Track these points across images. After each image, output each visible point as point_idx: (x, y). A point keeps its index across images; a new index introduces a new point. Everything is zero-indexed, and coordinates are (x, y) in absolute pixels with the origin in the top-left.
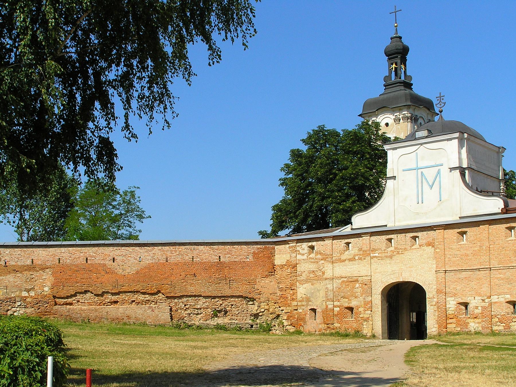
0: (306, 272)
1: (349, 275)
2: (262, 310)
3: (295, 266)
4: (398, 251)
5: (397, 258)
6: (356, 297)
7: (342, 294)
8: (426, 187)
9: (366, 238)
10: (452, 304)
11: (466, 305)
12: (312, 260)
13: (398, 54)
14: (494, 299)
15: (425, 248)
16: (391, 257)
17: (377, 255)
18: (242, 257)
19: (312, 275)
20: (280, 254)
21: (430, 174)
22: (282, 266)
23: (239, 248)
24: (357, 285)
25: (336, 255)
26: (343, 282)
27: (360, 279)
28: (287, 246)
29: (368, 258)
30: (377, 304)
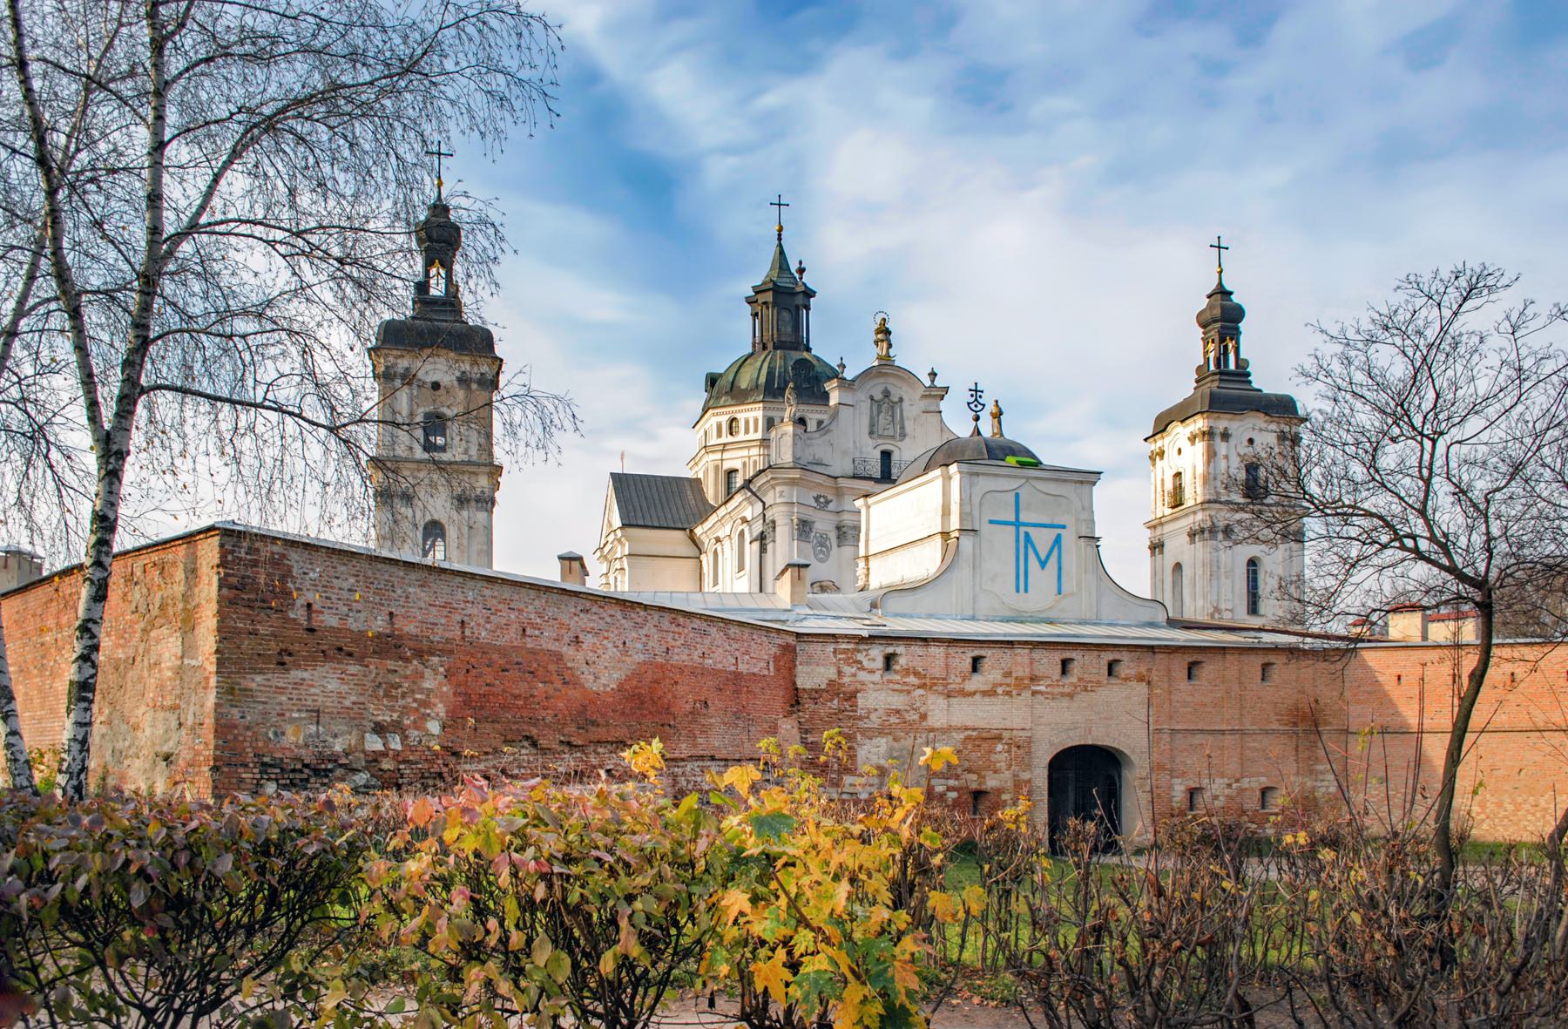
0: (881, 712)
1: (982, 724)
4: (1086, 687)
5: (1082, 698)
6: (995, 772)
7: (967, 765)
8: (1033, 563)
9: (1023, 652)
10: (1179, 791)
12: (896, 687)
14: (1245, 783)
15: (1134, 684)
16: (1071, 696)
17: (1042, 688)
19: (894, 720)
20: (808, 664)
21: (1043, 539)
22: (816, 694)
24: (1000, 747)
25: (955, 682)
26: (968, 738)
27: (1006, 734)
28: (830, 648)
29: (1027, 694)
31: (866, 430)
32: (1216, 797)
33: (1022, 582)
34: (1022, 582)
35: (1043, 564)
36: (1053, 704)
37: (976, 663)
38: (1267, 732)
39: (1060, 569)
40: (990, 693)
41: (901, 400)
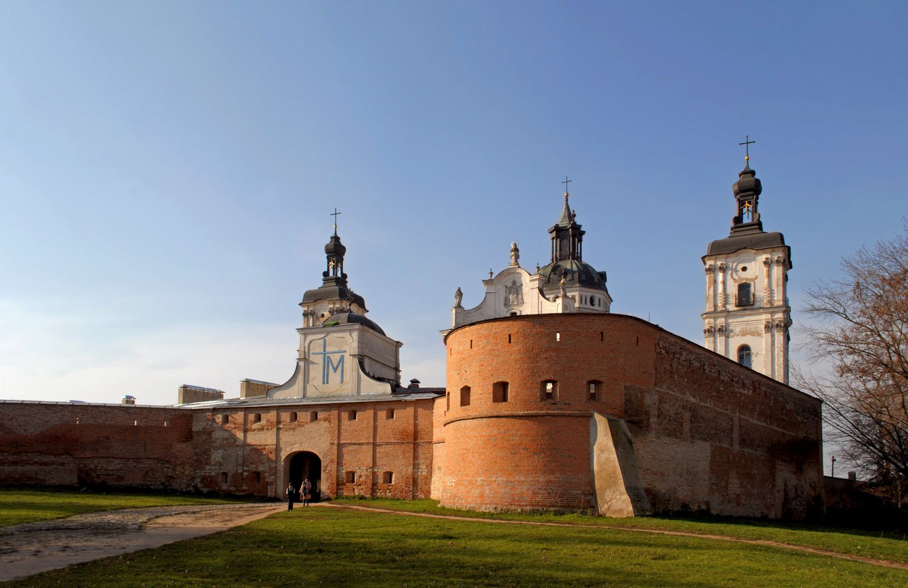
3: (210, 433)
5: (298, 430)
8: (331, 369)
11: (353, 473)
13: (336, 251)
16: (294, 429)
21: (335, 358)
22: (199, 433)
31: (502, 303)
32: (360, 476)
33: (326, 380)
34: (326, 380)
35: (335, 370)
37: (258, 419)
38: (387, 444)
39: (342, 371)
40: (261, 429)
41: (522, 285)
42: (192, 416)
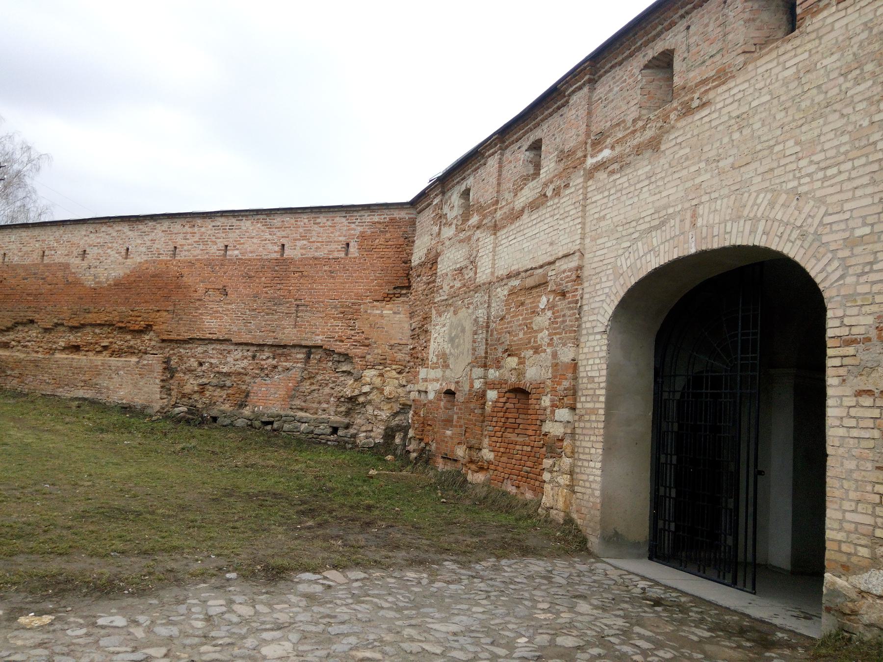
2: (366, 389)
16: (654, 145)
18: (333, 246)
23: (329, 223)
30: (591, 379)
36: (622, 180)
42: (413, 223)
